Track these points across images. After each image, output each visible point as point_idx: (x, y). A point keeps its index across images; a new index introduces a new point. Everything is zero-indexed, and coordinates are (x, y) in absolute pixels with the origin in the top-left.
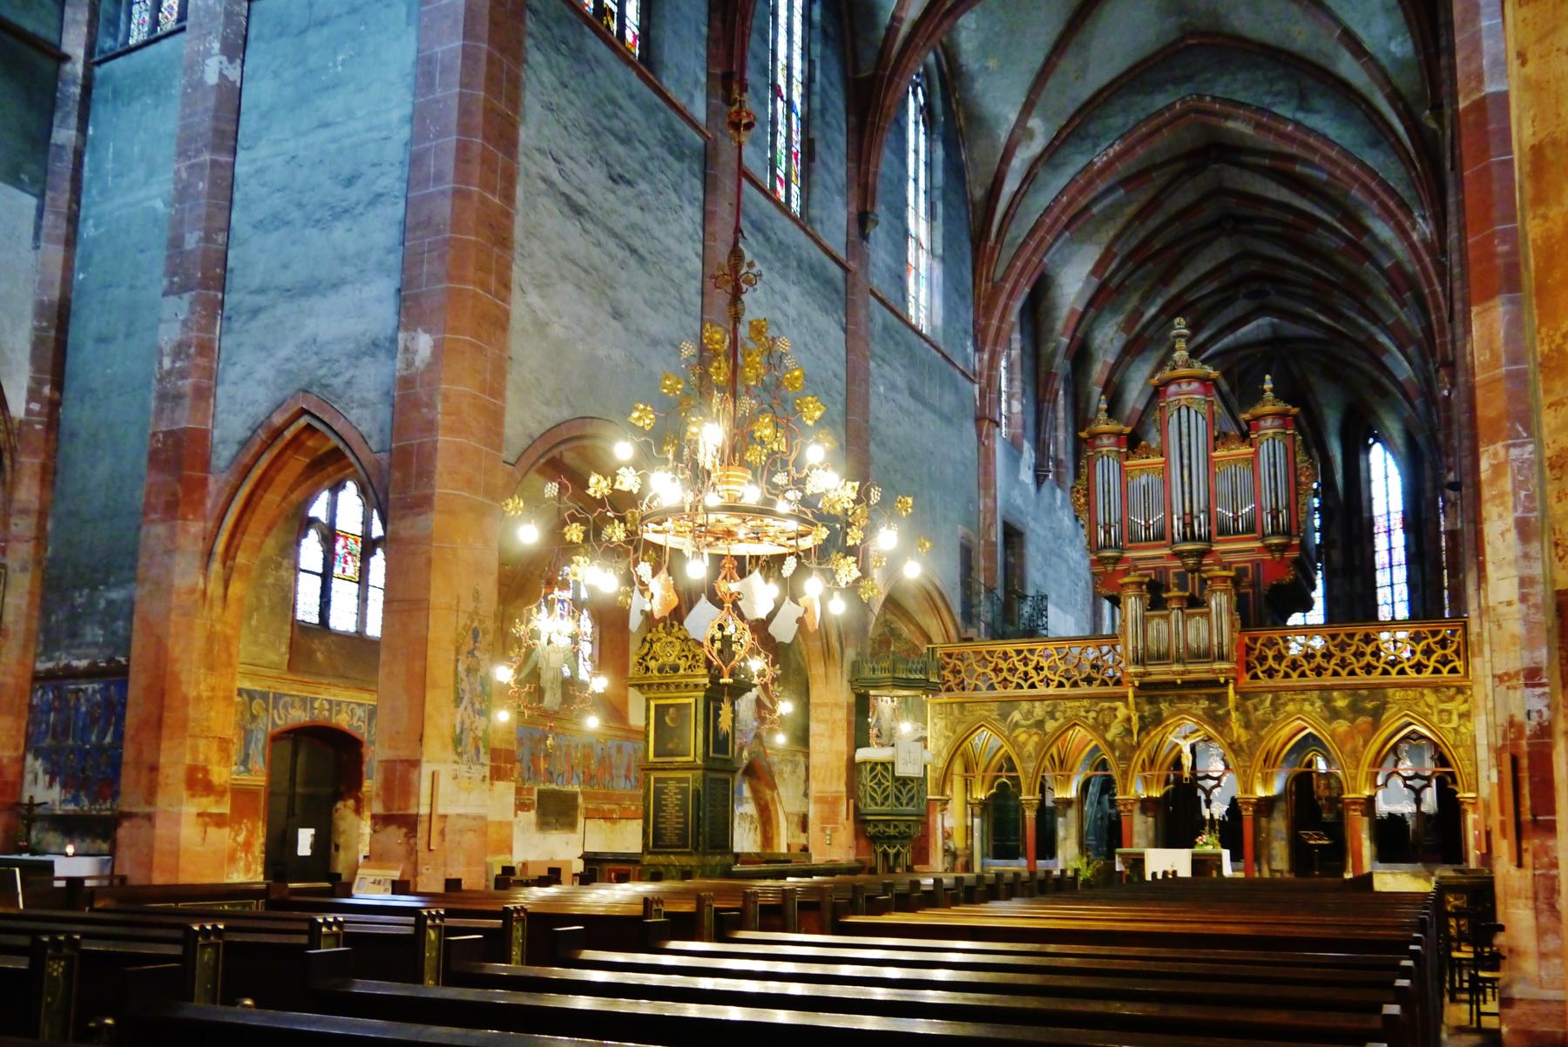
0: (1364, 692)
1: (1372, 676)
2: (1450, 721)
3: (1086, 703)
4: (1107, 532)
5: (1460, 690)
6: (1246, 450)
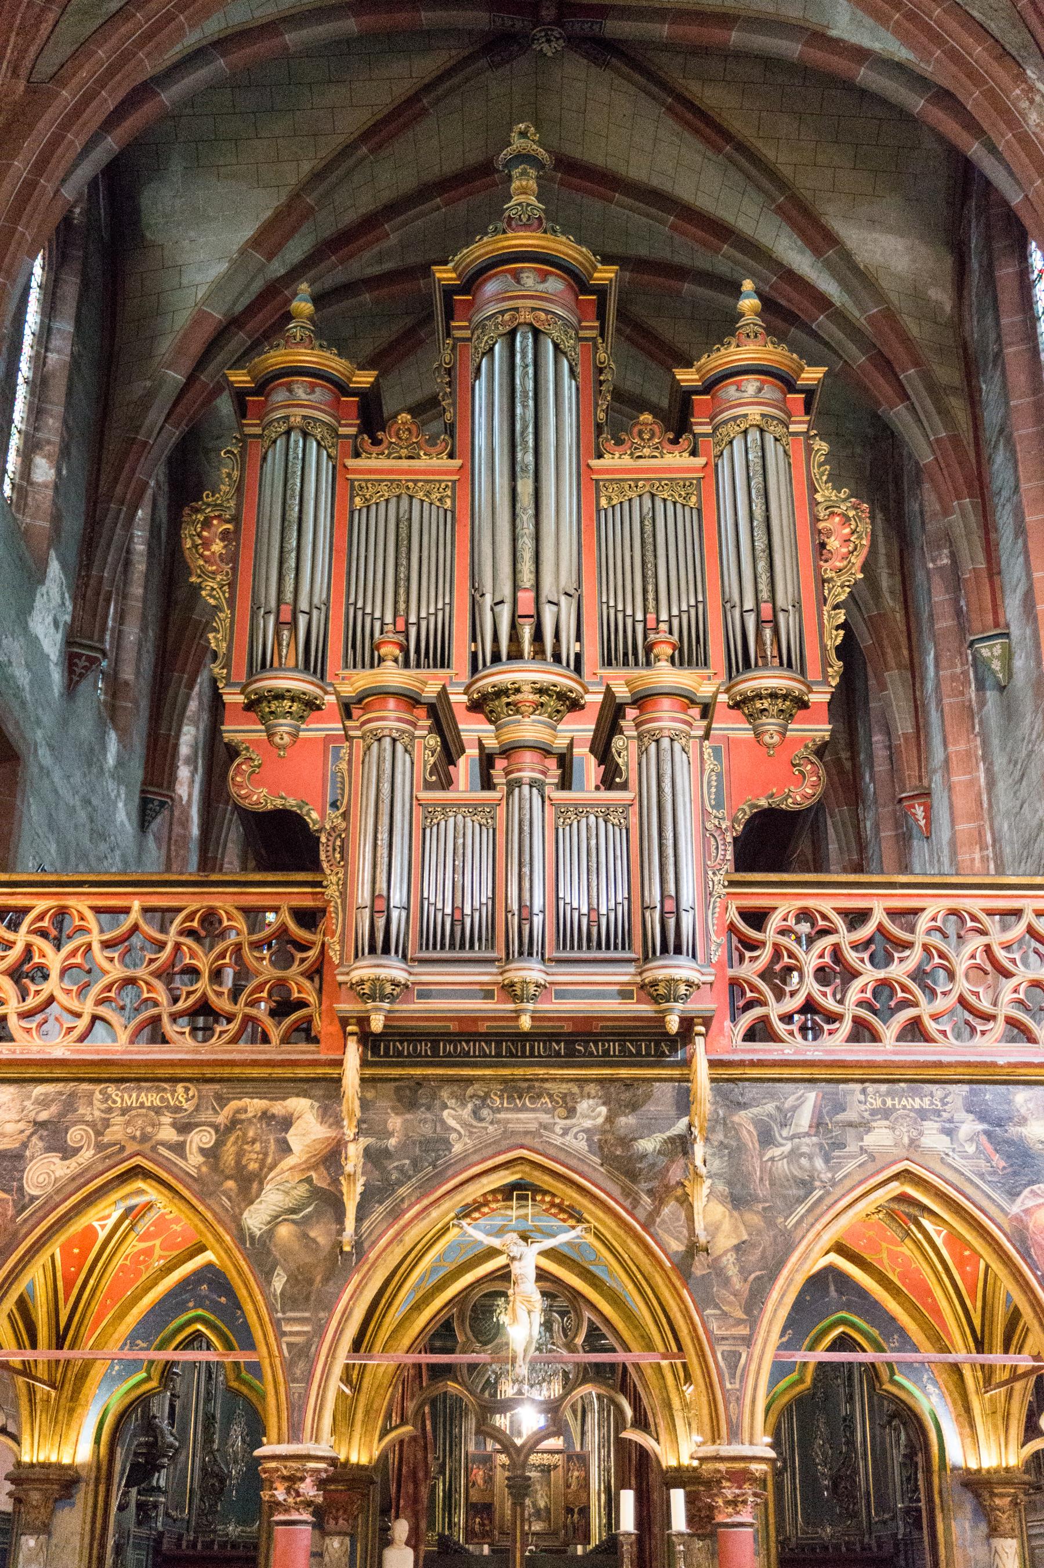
3: (180, 1095)
6: (677, 459)
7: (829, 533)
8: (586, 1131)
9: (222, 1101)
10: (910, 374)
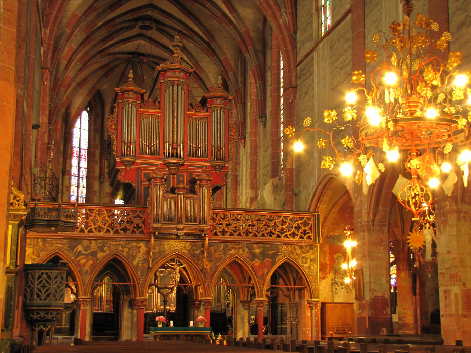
0: (269, 246)
1: (272, 238)
2: (306, 263)
3: (122, 243)
4: (129, 147)
5: (311, 248)
6: (203, 113)
7: (231, 131)
8: (188, 250)
9: (129, 244)
10: (250, 48)
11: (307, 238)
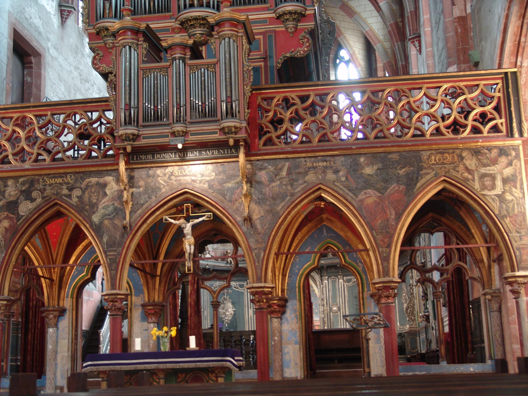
2: (493, 187)
3: (69, 179)
5: (503, 152)
8: (208, 181)
9: (83, 179)
11: (488, 132)
